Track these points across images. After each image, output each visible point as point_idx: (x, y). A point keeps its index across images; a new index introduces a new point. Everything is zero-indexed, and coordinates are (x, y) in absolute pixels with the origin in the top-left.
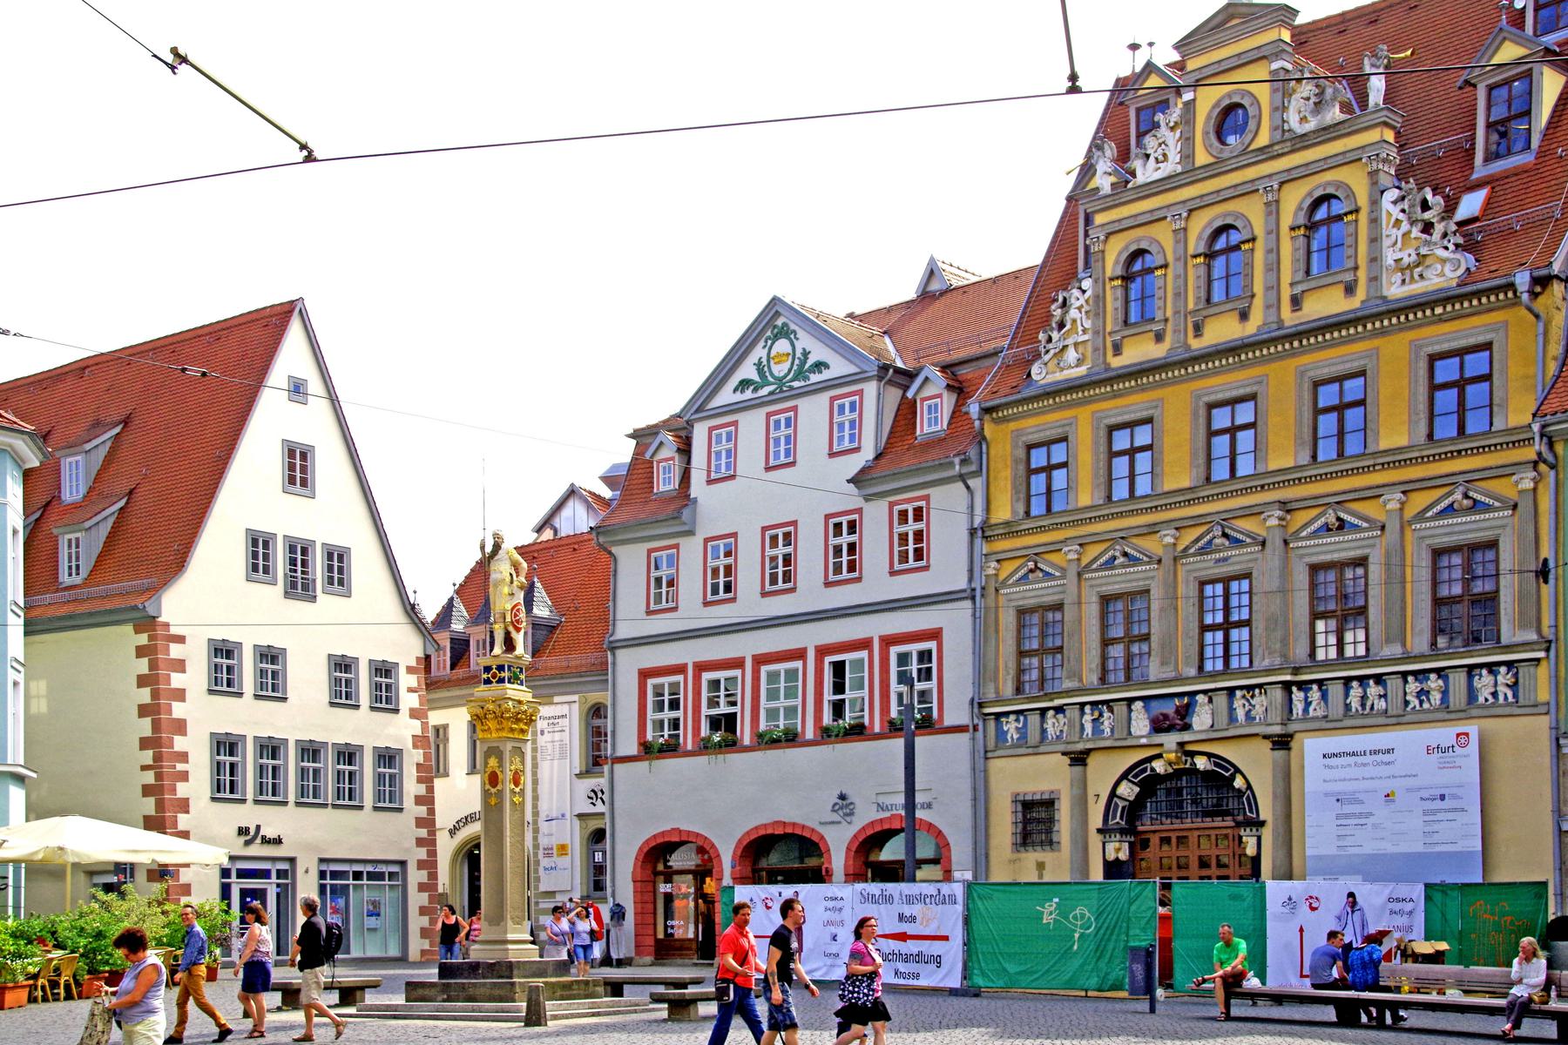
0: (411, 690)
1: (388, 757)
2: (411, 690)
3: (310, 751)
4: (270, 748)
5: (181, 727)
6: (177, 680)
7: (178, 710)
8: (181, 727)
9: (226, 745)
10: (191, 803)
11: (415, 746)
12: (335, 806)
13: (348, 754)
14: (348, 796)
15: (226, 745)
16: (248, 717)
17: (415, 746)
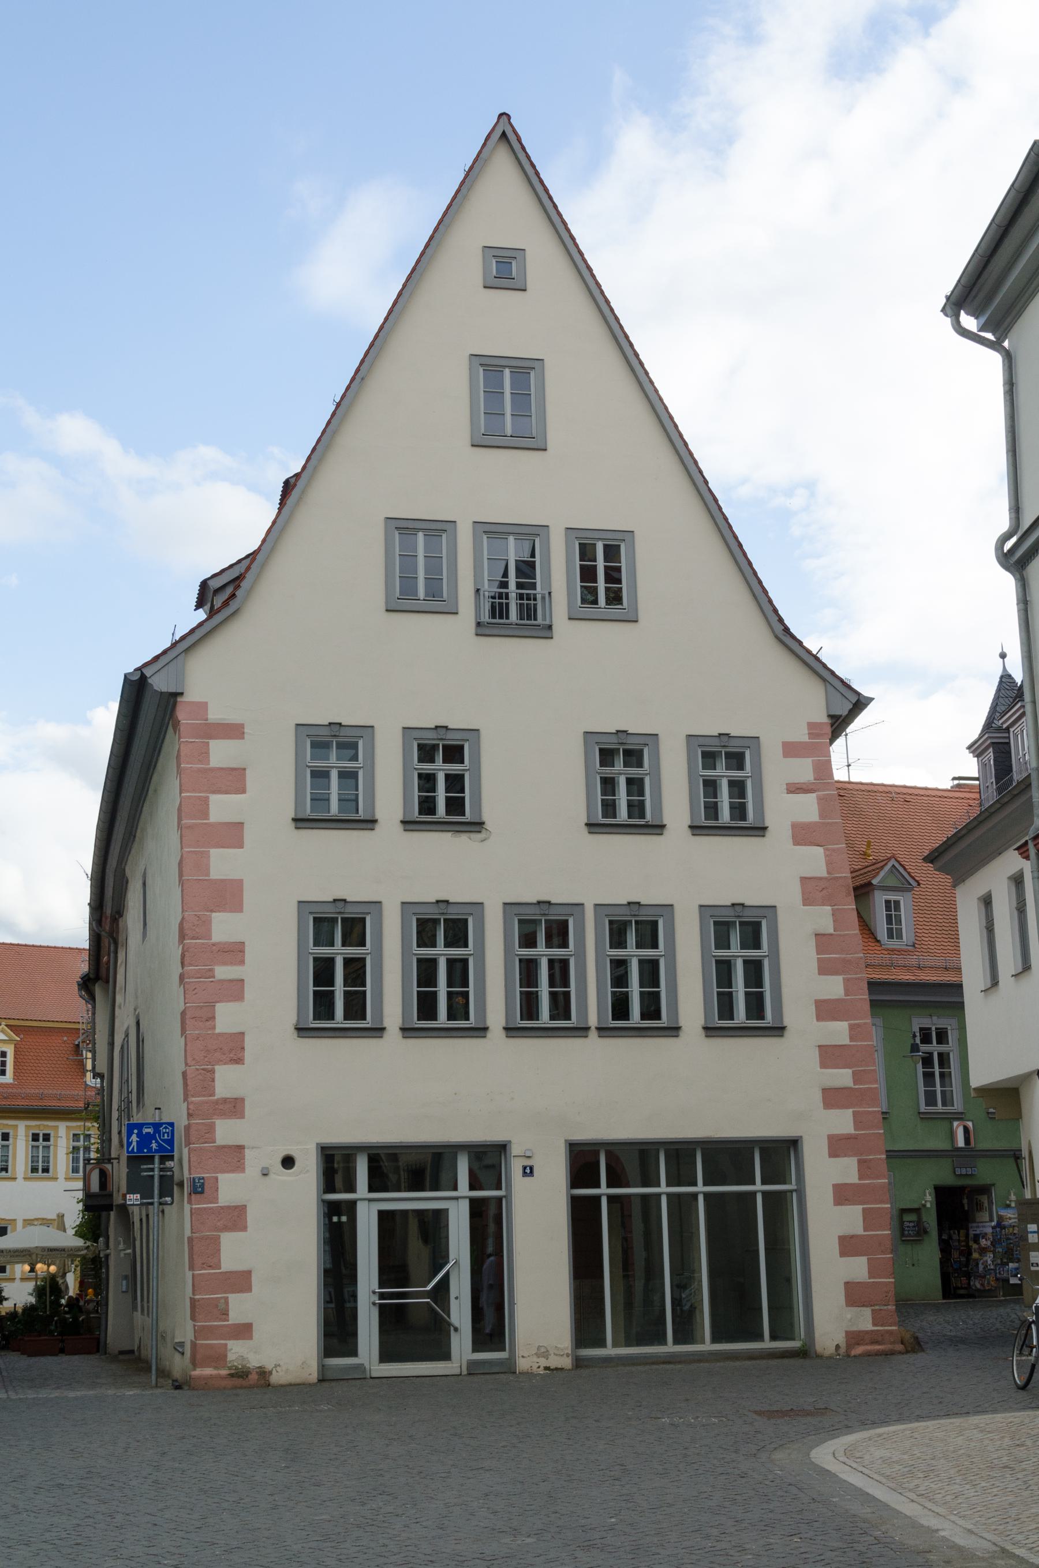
0: (795, 789)
1: (741, 932)
2: (795, 789)
3: (543, 927)
4: (443, 927)
5: (229, 896)
6: (222, 807)
7: (222, 863)
8: (229, 896)
9: (338, 926)
10: (248, 1042)
11: (807, 901)
12: (603, 1031)
13: (637, 927)
14: (639, 1007)
15: (338, 926)
16: (393, 869)
17: (807, 901)
